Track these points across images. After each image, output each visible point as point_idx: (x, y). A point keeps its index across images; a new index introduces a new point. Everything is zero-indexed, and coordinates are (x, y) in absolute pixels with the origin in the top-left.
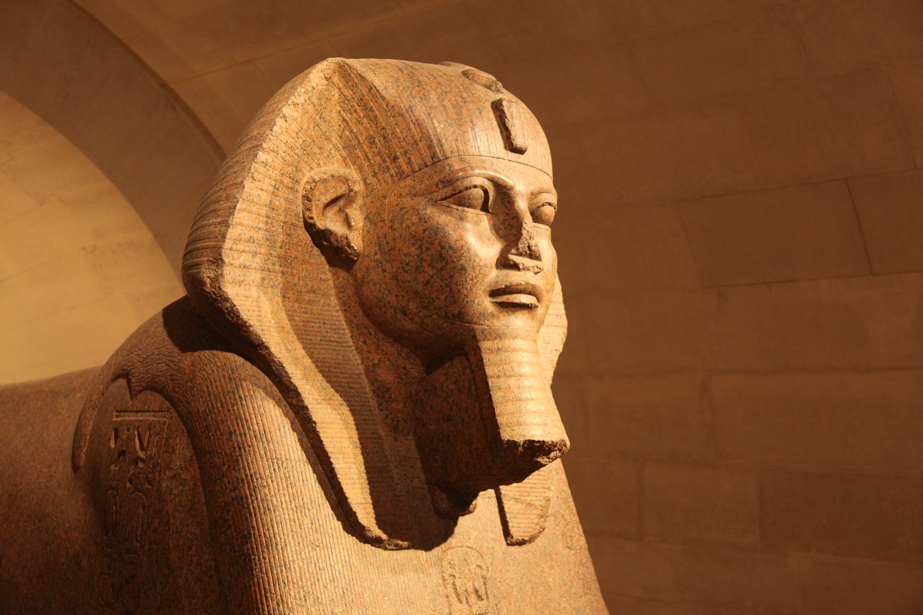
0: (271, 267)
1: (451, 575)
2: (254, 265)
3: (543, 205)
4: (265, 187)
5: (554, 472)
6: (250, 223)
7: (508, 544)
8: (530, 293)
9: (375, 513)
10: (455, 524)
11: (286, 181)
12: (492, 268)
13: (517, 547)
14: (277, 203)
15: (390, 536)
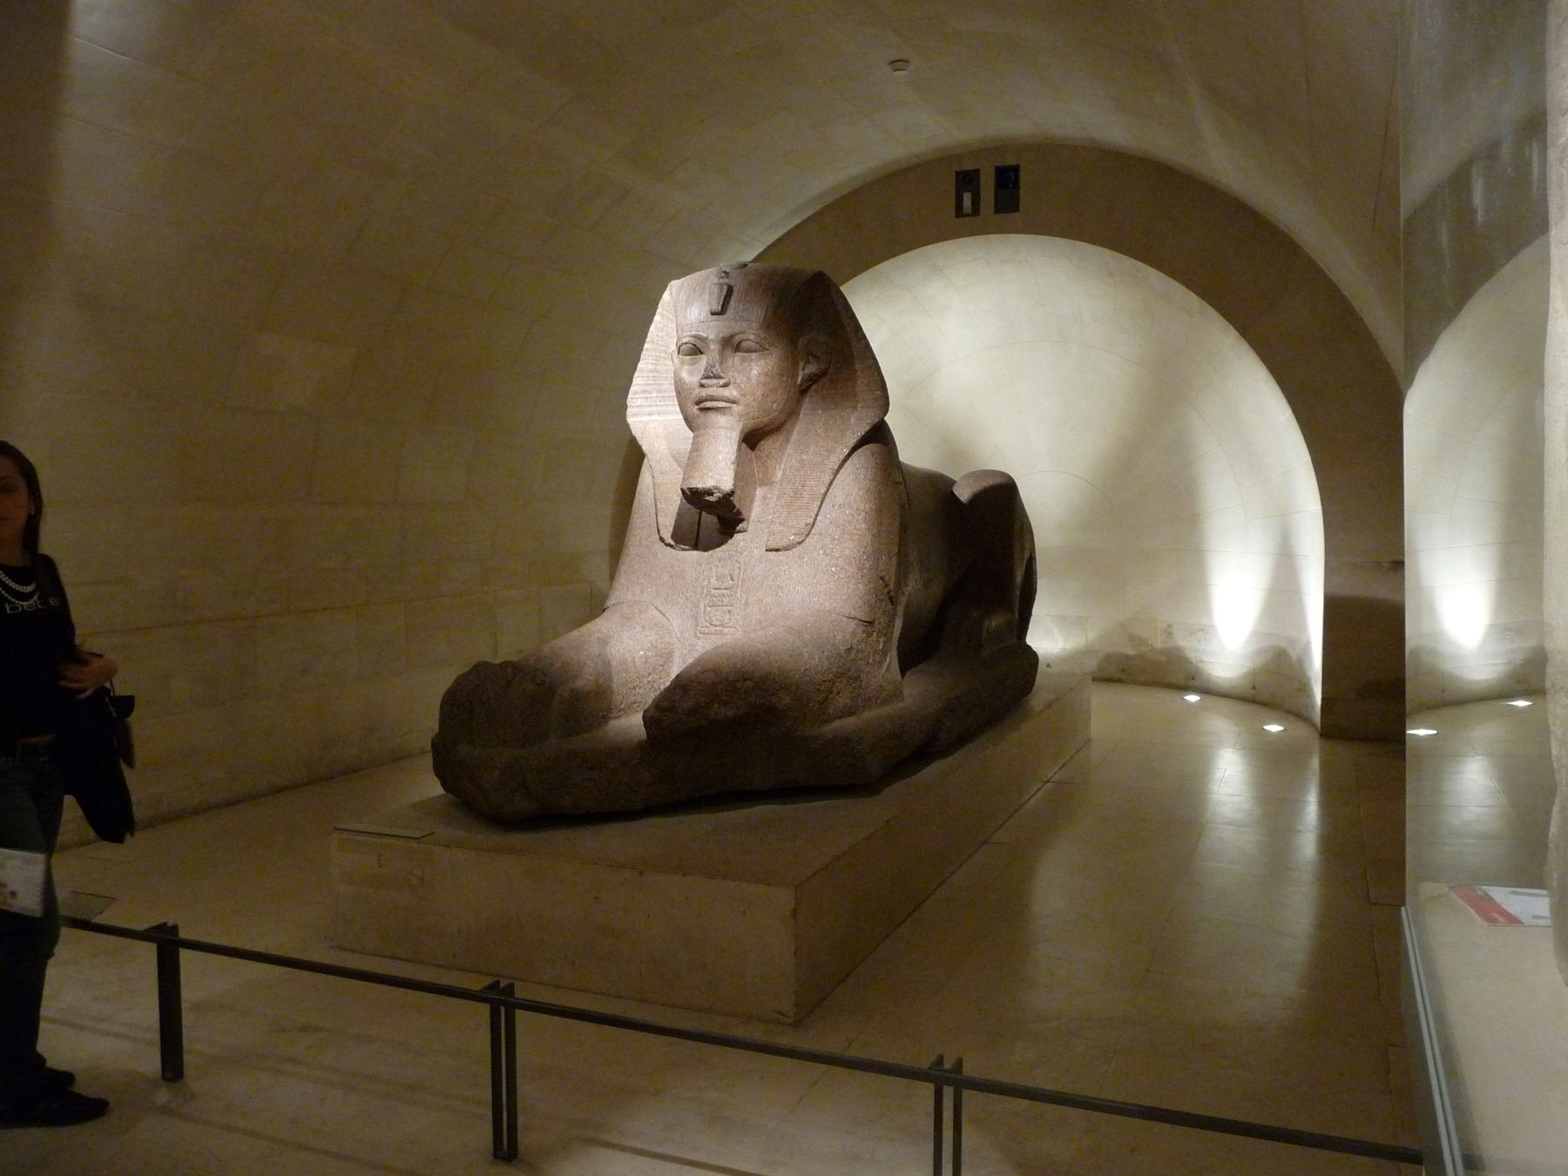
0: (659, 403)
1: (716, 566)
2: (646, 404)
3: (740, 342)
4: (650, 361)
5: (836, 507)
6: (643, 382)
7: (767, 550)
8: (711, 400)
9: (674, 530)
10: (731, 536)
11: (663, 355)
12: (694, 389)
13: (775, 553)
14: (660, 368)
15: (676, 542)
